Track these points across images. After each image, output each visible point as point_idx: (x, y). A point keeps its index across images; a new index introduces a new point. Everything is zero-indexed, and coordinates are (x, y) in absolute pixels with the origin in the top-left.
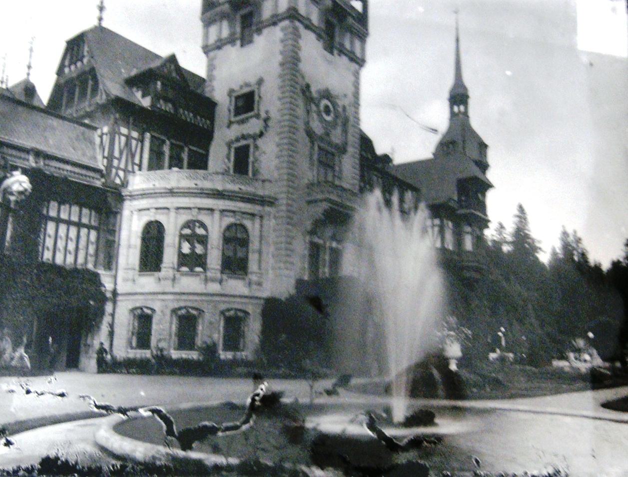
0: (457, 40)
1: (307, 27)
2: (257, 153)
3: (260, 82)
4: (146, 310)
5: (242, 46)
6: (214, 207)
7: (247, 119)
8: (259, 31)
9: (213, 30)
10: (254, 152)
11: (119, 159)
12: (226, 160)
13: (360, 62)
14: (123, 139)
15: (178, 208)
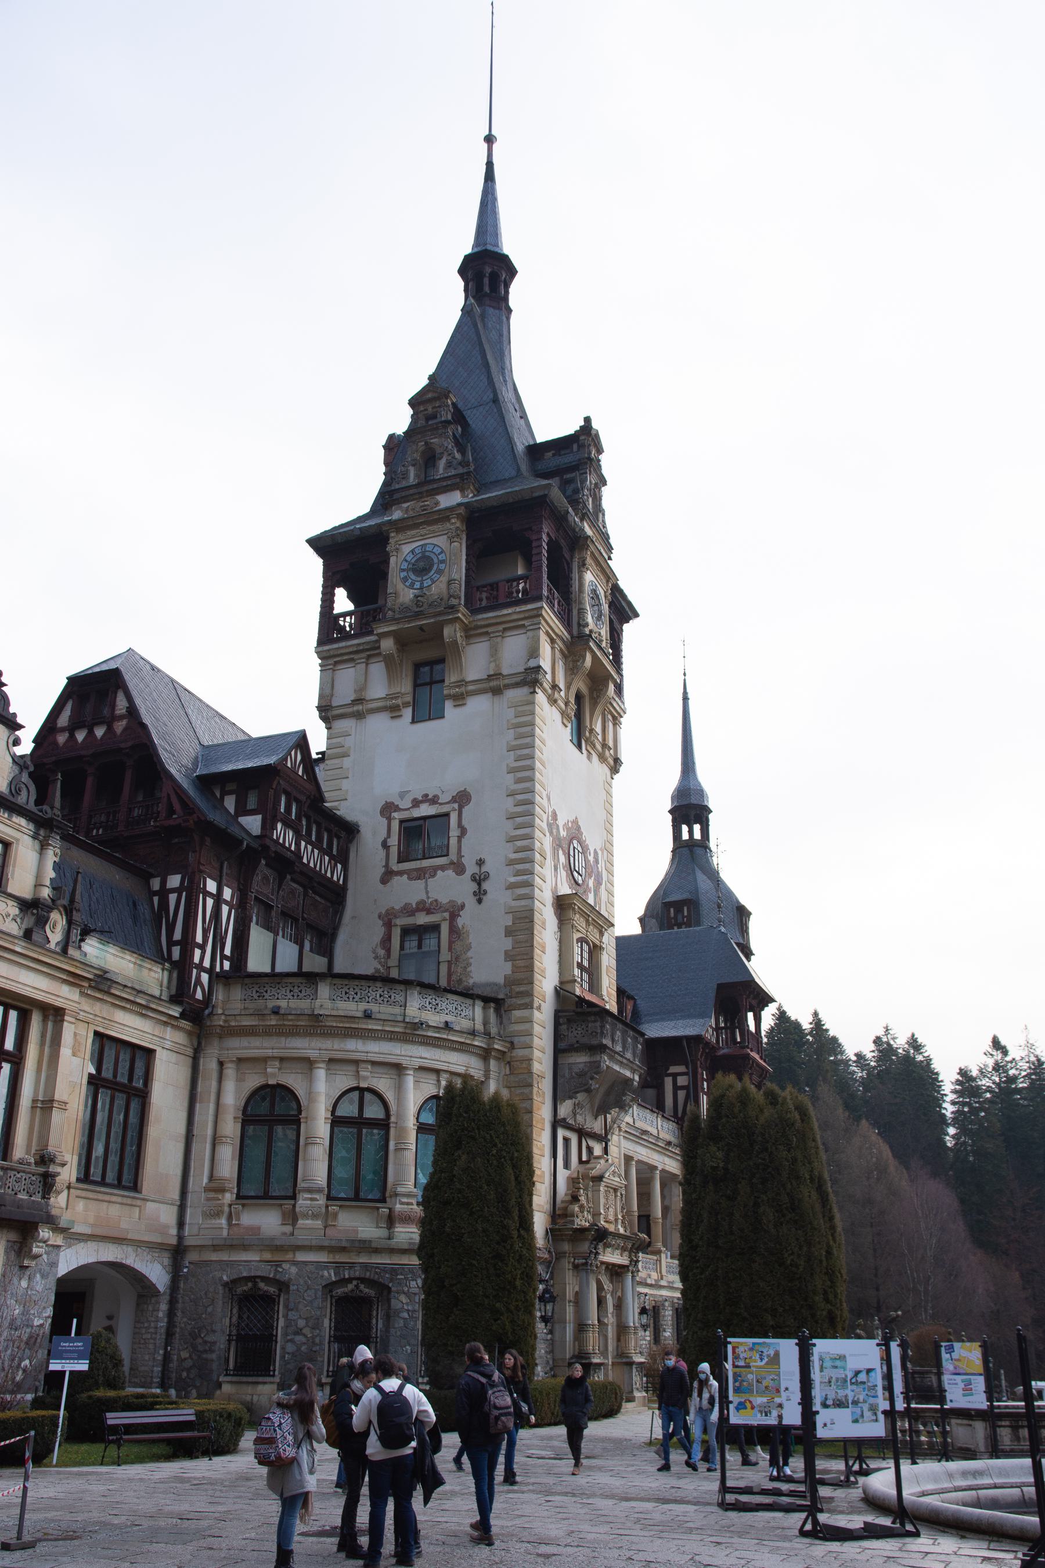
0: (685, 699)
1: (553, 701)
2: (458, 946)
3: (462, 798)
4: (262, 1285)
5: (414, 721)
6: (404, 1062)
7: (434, 871)
8: (459, 699)
9: (348, 677)
10: (451, 943)
11: (202, 947)
12: (382, 952)
13: (615, 766)
14: (210, 902)
15: (331, 1061)
